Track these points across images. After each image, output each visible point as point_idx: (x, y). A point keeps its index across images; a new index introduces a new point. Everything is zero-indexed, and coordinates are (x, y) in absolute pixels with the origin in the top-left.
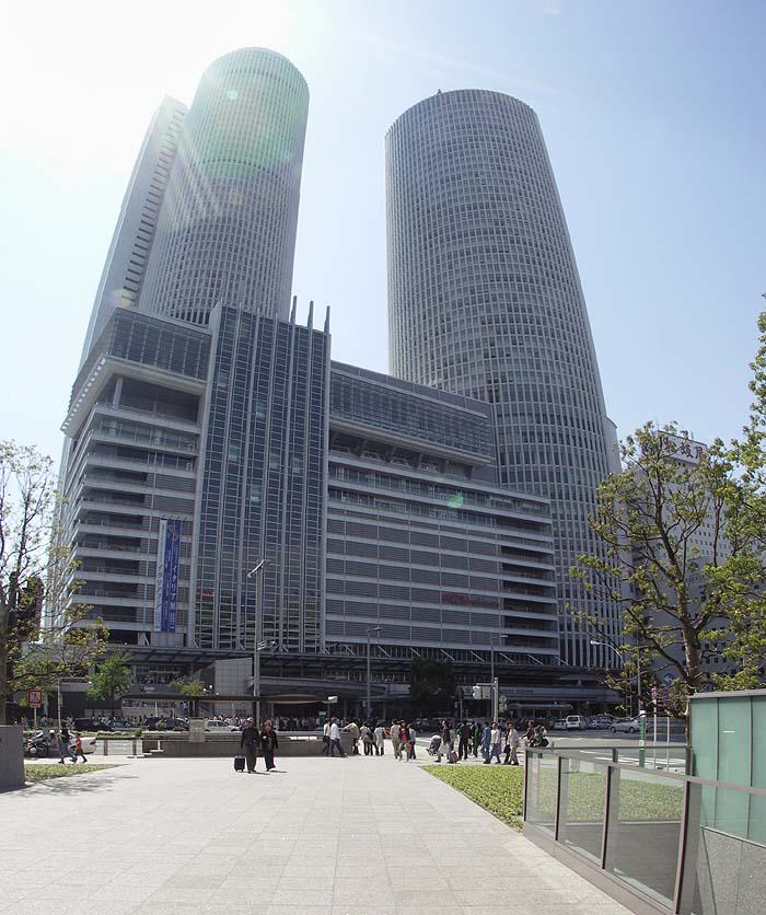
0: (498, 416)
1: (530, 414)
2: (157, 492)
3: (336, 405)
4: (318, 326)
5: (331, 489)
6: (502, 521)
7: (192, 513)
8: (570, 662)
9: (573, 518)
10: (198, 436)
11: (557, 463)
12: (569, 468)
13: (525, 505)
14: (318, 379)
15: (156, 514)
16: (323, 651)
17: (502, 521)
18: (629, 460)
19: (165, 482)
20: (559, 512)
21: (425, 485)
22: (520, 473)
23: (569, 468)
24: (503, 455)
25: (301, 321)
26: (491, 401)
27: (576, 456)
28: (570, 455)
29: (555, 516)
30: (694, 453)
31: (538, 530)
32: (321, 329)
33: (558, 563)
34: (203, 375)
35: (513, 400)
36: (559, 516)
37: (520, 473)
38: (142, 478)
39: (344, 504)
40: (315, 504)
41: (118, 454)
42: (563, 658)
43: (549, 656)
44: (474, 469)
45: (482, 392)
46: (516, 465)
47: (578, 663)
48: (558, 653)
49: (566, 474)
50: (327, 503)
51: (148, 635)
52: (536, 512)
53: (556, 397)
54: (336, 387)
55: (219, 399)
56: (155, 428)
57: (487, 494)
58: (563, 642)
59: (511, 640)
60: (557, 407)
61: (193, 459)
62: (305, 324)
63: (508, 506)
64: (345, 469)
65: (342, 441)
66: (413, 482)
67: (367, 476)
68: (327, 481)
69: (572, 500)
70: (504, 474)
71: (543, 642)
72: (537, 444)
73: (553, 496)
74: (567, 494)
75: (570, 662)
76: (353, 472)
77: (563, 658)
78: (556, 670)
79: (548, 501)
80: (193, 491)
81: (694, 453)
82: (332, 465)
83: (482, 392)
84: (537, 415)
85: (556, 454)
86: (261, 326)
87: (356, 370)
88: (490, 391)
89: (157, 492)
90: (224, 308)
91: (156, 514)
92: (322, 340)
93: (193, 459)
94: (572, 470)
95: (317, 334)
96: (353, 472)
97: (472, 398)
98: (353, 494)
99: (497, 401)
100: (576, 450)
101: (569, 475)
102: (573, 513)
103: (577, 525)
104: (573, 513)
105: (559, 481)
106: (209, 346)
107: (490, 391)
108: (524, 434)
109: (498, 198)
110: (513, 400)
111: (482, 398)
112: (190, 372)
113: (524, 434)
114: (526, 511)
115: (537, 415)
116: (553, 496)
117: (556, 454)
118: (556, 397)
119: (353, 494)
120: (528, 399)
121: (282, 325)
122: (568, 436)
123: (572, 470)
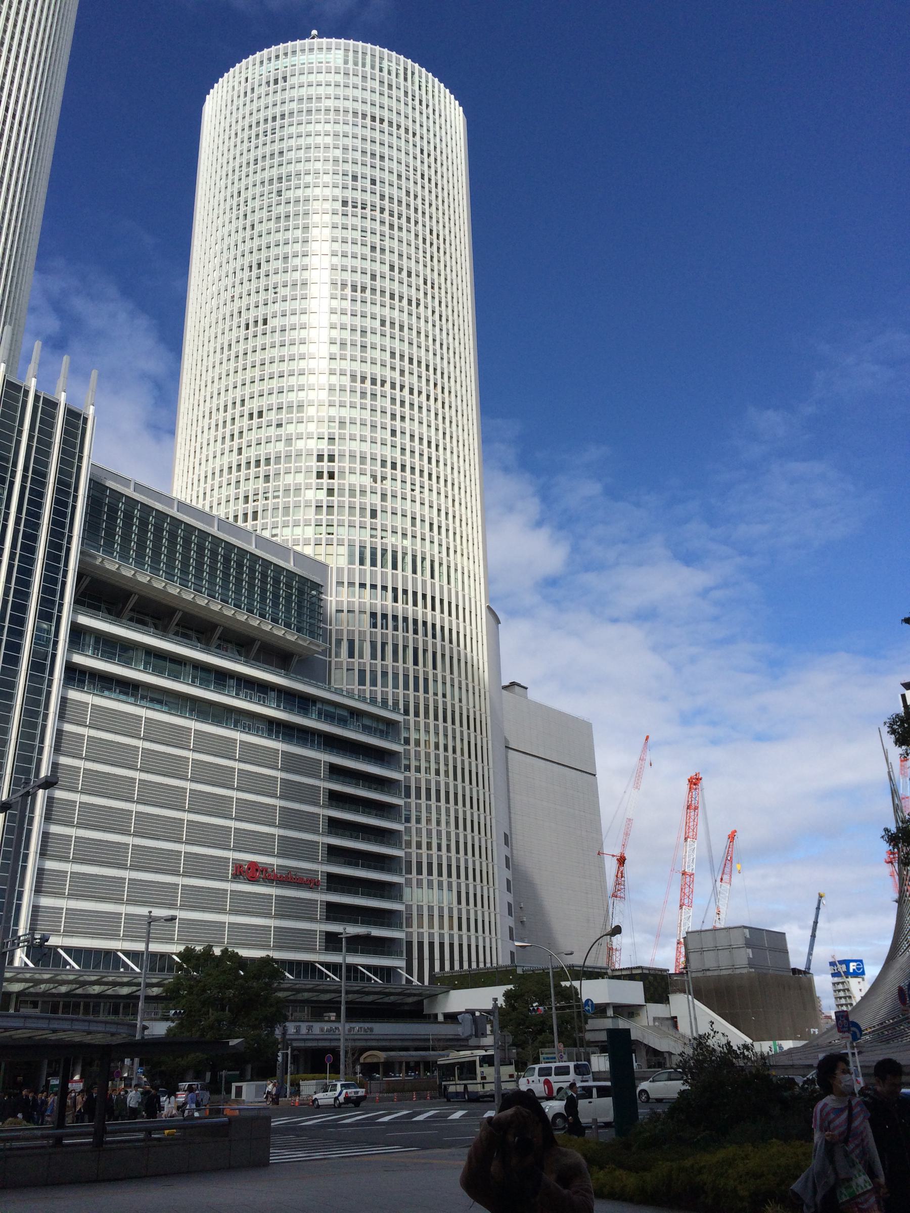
1: (384, 588)
8: (421, 978)
11: (416, 663)
13: (367, 722)
20: (413, 736)
42: (409, 971)
48: (402, 963)
49: (426, 680)
52: (383, 735)
57: (314, 700)
58: (409, 944)
59: (332, 941)
63: (342, 722)
73: (406, 712)
75: (421, 978)
79: (399, 718)
82: (78, 634)
84: (395, 590)
85: (416, 650)
94: (435, 675)
104: (433, 739)
105: (416, 689)
114: (367, 729)
115: (395, 590)
117: (416, 650)
123: (435, 675)
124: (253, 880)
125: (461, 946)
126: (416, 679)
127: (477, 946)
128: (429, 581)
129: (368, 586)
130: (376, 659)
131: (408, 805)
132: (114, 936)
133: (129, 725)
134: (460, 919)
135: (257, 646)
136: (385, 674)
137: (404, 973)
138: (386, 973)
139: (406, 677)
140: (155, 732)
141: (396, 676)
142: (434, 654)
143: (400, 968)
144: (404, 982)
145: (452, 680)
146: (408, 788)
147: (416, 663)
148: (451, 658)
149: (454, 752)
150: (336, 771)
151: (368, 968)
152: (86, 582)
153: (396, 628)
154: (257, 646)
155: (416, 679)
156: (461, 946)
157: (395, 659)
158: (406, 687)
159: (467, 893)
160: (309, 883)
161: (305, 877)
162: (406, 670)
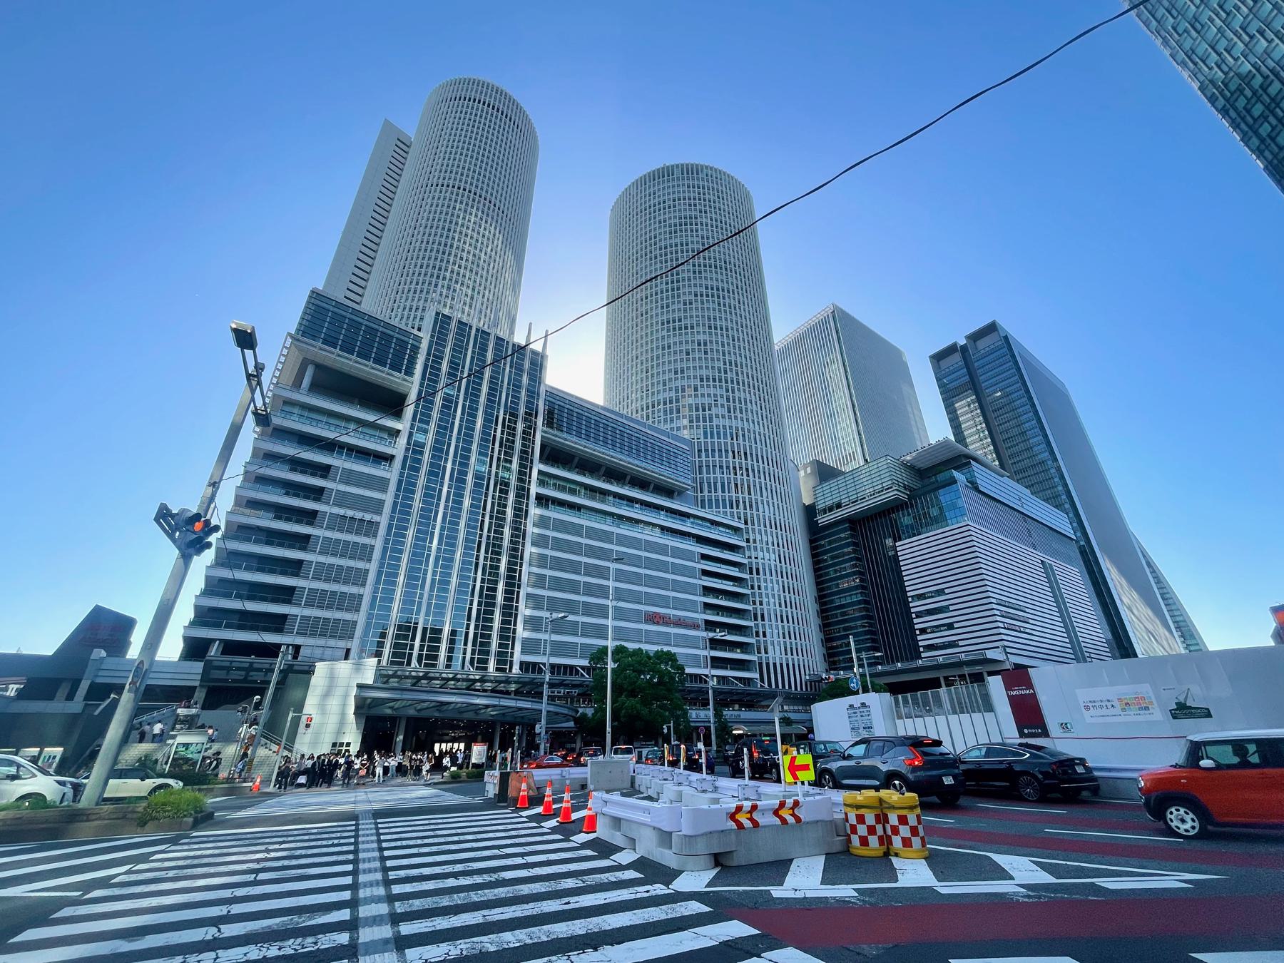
0: (699, 451)
2: (342, 488)
3: (549, 422)
4: (537, 347)
6: (701, 540)
13: (721, 529)
14: (532, 394)
16: (516, 669)
17: (701, 540)
19: (350, 477)
21: (631, 500)
22: (717, 501)
23: (760, 499)
25: (519, 339)
29: (748, 541)
33: (752, 587)
34: (409, 372)
35: (712, 437)
36: (751, 541)
37: (717, 501)
38: (324, 470)
39: (554, 514)
40: (520, 513)
41: (298, 443)
42: (762, 681)
43: (749, 679)
44: (676, 494)
48: (757, 676)
49: (757, 503)
50: (534, 511)
51: (297, 648)
58: (760, 664)
65: (553, 454)
73: (746, 523)
74: (759, 521)
76: (563, 484)
77: (762, 681)
78: (758, 694)
79: (743, 526)
80: (385, 491)
86: (476, 336)
87: (572, 396)
89: (342, 488)
93: (389, 458)
94: (762, 501)
95: (534, 352)
96: (563, 484)
98: (561, 503)
102: (765, 539)
104: (765, 539)
106: (415, 349)
110: (712, 437)
112: (396, 367)
116: (746, 523)
118: (750, 438)
119: (561, 503)
120: (725, 437)
122: (759, 471)
124: (657, 623)
125: (793, 665)
131: (752, 579)
132: (575, 657)
133: (577, 530)
138: (747, 681)
140: (592, 534)
146: (751, 569)
147: (750, 494)
149: (778, 546)
150: (704, 557)
151: (736, 678)
152: (547, 451)
156: (793, 665)
160: (695, 626)
161: (690, 621)
162: (744, 498)
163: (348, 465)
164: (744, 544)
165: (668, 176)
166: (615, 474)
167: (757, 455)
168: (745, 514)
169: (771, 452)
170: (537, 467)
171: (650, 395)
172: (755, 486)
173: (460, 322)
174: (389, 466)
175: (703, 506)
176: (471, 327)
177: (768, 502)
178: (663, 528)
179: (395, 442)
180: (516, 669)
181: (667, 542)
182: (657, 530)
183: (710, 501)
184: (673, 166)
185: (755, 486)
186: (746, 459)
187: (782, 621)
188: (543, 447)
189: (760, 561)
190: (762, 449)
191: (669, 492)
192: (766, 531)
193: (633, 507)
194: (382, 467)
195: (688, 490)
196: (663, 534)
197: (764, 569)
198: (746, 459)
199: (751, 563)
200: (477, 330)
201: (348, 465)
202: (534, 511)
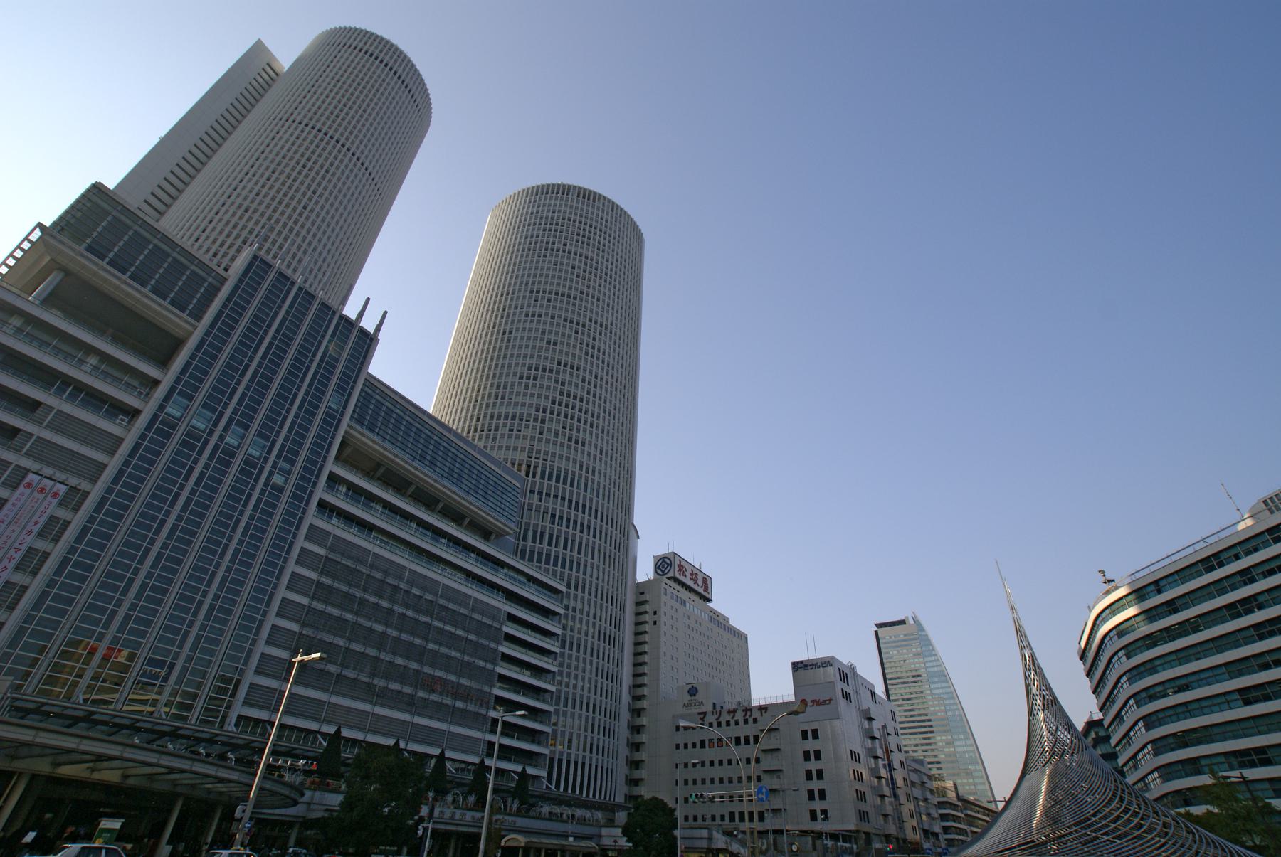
0: (531, 491)
1: (563, 499)
2: (48, 435)
3: (359, 418)
4: (368, 324)
5: (323, 505)
6: (512, 597)
7: (94, 482)
8: (558, 786)
9: (585, 613)
10: (156, 383)
11: (579, 553)
12: (590, 561)
15: (26, 463)
16: (230, 726)
17: (512, 597)
18: (644, 571)
20: (572, 604)
21: (438, 533)
23: (590, 561)
24: (526, 531)
25: (350, 311)
26: (527, 475)
27: (599, 551)
28: (593, 549)
29: (567, 608)
30: (700, 582)
31: (548, 618)
32: (371, 329)
37: (540, 554)
39: (334, 527)
42: (550, 780)
44: (494, 536)
45: (520, 465)
46: (537, 545)
47: (574, 790)
48: (544, 774)
49: (585, 566)
50: (312, 517)
53: (592, 489)
54: (365, 397)
55: (208, 349)
56: (91, 350)
58: (552, 760)
60: (591, 500)
61: (135, 413)
62: (353, 317)
64: (348, 489)
66: (424, 527)
67: (372, 504)
68: (320, 493)
69: (586, 596)
70: (524, 551)
71: (529, 757)
72: (564, 528)
74: (584, 588)
75: (558, 786)
76: (356, 492)
79: (564, 589)
80: (112, 453)
81: (700, 582)
82: (334, 479)
83: (520, 465)
84: (570, 501)
85: (580, 544)
88: (529, 466)
90: (255, 257)
91: (26, 463)
92: (367, 342)
93: (135, 413)
94: (592, 564)
95: (363, 332)
96: (356, 492)
97: (509, 465)
98: (349, 519)
99: (534, 476)
100: (600, 545)
101: (589, 569)
102: (586, 609)
103: (587, 622)
104: (586, 609)
105: (578, 571)
106: (213, 292)
107: (529, 466)
108: (553, 516)
109: (587, 295)
111: (520, 470)
112: (179, 305)
113: (553, 516)
115: (570, 501)
116: (569, 586)
117: (580, 544)
118: (592, 489)
119: (349, 519)
121: (324, 306)
122: (595, 529)
123: (592, 564)
125: (590, 765)
126: (579, 564)
127: (602, 767)
128: (595, 499)
129: (552, 496)
130: (549, 565)
134: (592, 745)
135: (467, 520)
136: (556, 558)
137: (545, 781)
139: (571, 562)
141: (564, 559)
142: (593, 548)
143: (544, 778)
144: (544, 787)
145: (604, 569)
147: (579, 553)
148: (605, 554)
153: (568, 527)
154: (467, 520)
155: (579, 564)
156: (590, 765)
157: (565, 548)
158: (571, 569)
159: (599, 726)
162: (572, 557)
163: (68, 408)
164: (561, 611)
165: (563, 194)
166: (427, 499)
167: (596, 511)
168: (570, 576)
169: (613, 510)
170: (330, 466)
171: (510, 347)
172: (587, 545)
173: (281, 274)
174: (129, 423)
175: (522, 557)
176: (293, 283)
177: (598, 567)
178: (470, 575)
179: (148, 394)
180: (230, 726)
181: (469, 592)
182: (461, 576)
183: (532, 552)
184: (569, 186)
185: (587, 545)
186: (584, 513)
187: (587, 710)
188: (344, 443)
189: (576, 635)
190: (603, 505)
191: (486, 533)
192: (589, 601)
193: (438, 541)
194: (118, 421)
195: (508, 534)
196: (467, 581)
197: (579, 645)
198: (584, 513)
199: (564, 635)
200: (300, 289)
201: (68, 408)
202: (312, 517)
